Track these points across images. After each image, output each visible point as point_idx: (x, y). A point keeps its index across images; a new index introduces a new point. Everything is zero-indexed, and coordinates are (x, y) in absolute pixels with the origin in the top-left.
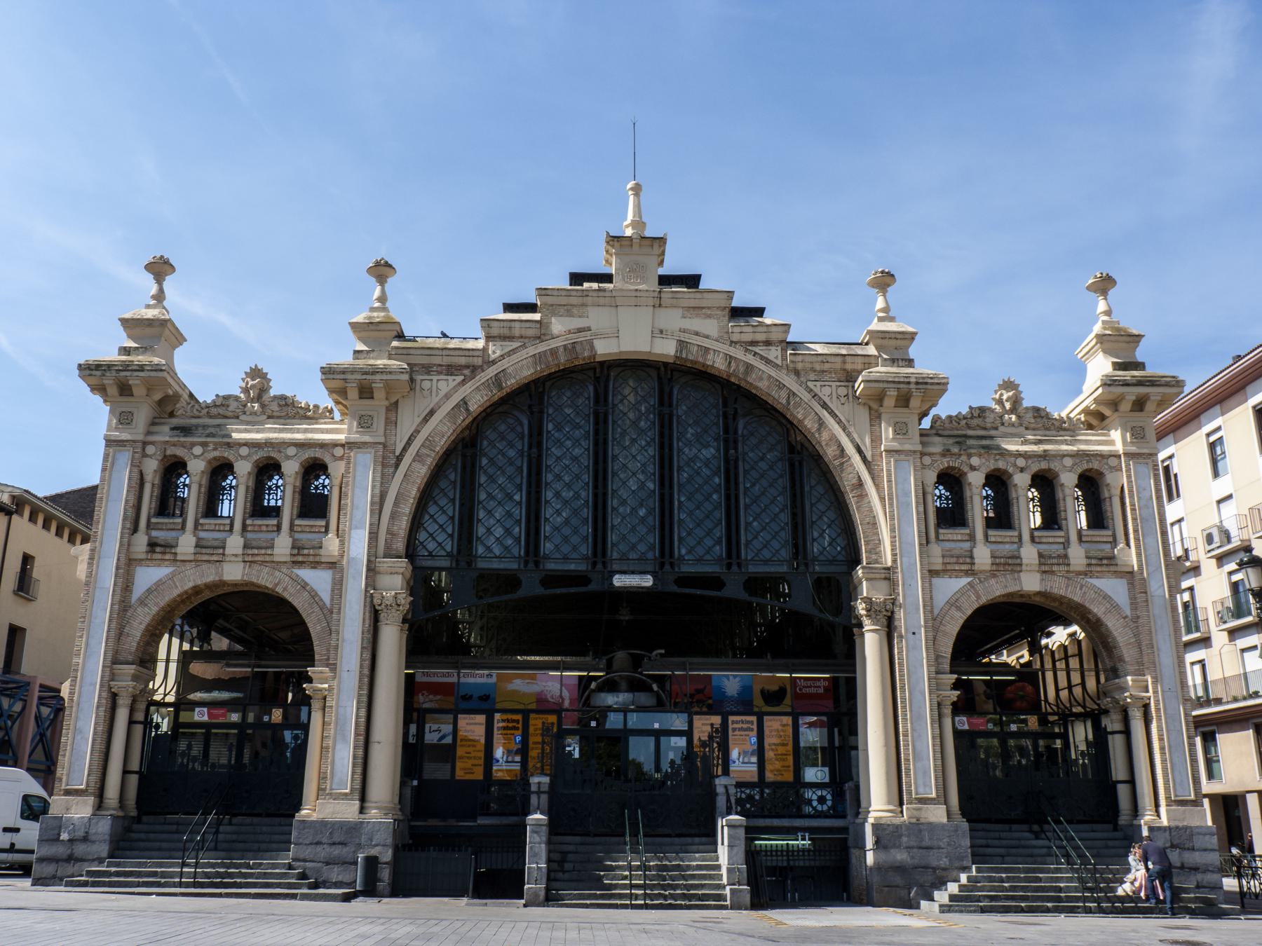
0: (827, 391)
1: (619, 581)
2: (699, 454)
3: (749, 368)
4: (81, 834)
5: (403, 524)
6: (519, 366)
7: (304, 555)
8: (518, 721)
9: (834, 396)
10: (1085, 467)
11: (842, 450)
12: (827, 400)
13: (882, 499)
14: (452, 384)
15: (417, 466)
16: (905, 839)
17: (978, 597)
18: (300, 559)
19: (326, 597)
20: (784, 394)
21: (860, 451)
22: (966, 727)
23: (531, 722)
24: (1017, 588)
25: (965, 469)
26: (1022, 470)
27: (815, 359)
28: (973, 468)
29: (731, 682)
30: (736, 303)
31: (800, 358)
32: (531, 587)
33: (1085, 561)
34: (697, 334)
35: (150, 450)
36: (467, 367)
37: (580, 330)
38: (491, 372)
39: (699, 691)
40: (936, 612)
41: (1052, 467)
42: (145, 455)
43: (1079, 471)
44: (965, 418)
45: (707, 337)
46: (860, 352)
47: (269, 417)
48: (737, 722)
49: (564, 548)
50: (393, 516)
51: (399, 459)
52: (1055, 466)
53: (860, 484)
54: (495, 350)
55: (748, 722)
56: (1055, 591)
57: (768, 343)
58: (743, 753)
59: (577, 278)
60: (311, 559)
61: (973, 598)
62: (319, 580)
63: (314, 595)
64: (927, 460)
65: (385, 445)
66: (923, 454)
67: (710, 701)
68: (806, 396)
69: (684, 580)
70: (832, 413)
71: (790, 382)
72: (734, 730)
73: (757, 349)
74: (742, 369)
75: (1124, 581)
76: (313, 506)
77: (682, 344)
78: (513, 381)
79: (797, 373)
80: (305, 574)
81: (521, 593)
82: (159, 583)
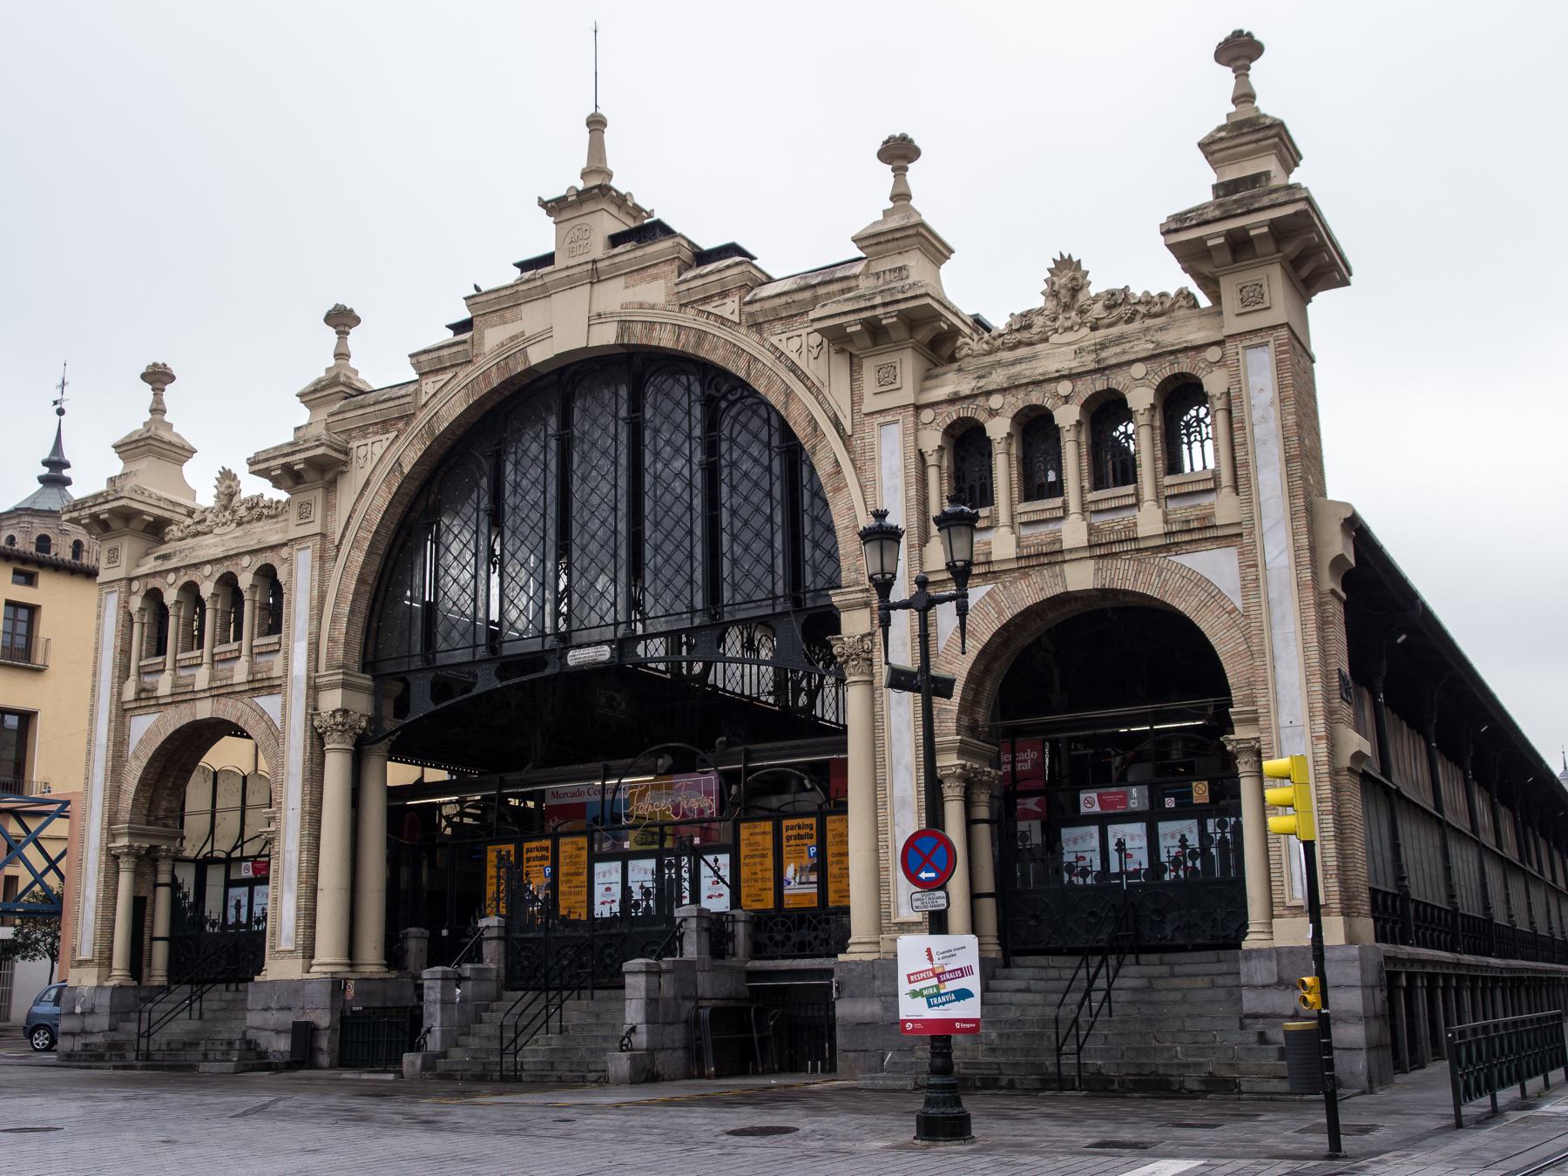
0: (795, 343)
1: (575, 657)
2: (674, 467)
3: (702, 335)
4: (88, 1006)
6: (449, 403)
8: (546, 849)
9: (804, 349)
10: (1167, 372)
11: (816, 426)
12: (794, 356)
13: (862, 488)
14: (386, 444)
15: (355, 553)
16: (878, 983)
17: (1000, 613)
18: (257, 685)
20: (743, 363)
21: (837, 424)
22: (1097, 808)
23: (562, 848)
24: (1059, 590)
25: (981, 416)
26: (1067, 399)
27: (777, 302)
28: (993, 413)
30: (706, 244)
31: (756, 307)
32: (488, 681)
33: (1159, 528)
34: (641, 306)
35: (135, 586)
36: (401, 418)
37: (512, 339)
38: (422, 417)
41: (1114, 385)
42: (130, 593)
43: (1157, 381)
45: (653, 307)
46: (848, 273)
48: (792, 828)
50: (334, 620)
51: (338, 547)
52: (1118, 381)
53: (838, 470)
54: (429, 386)
55: (806, 826)
56: (1118, 585)
57: (724, 294)
58: (800, 870)
59: (524, 266)
61: (994, 614)
62: (270, 704)
64: (927, 415)
65: (323, 535)
66: (918, 408)
68: (767, 358)
70: (802, 377)
71: (748, 341)
72: (789, 838)
73: (708, 308)
74: (692, 340)
75: (1233, 551)
76: (273, 621)
77: (624, 325)
78: (446, 424)
79: (757, 326)
82: (149, 731)
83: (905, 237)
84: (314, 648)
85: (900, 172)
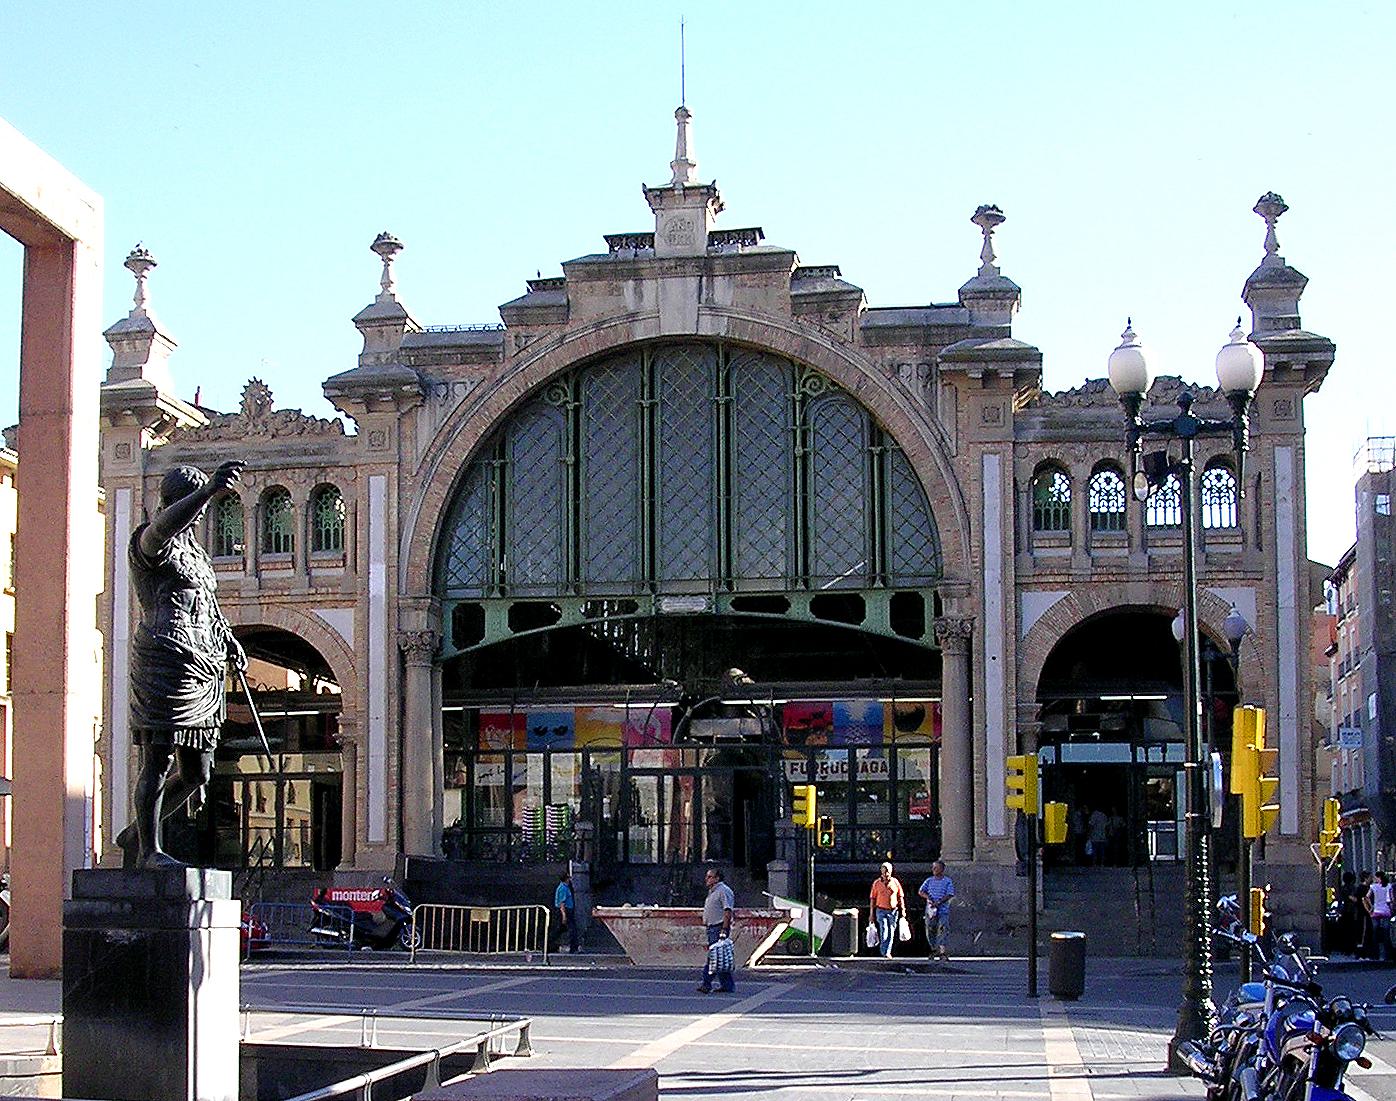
1: (667, 606)
5: (425, 553)
7: (318, 595)
19: (349, 636)
29: (857, 707)
32: (571, 615)
39: (817, 715)
40: (1025, 632)
44: (1078, 393)
47: (273, 436)
49: (611, 568)
60: (331, 597)
62: (343, 620)
63: (337, 637)
67: (831, 728)
69: (739, 603)
76: (324, 538)
80: (325, 614)
81: (560, 623)
83: (994, 292)
84: (395, 572)
85: (988, 234)
